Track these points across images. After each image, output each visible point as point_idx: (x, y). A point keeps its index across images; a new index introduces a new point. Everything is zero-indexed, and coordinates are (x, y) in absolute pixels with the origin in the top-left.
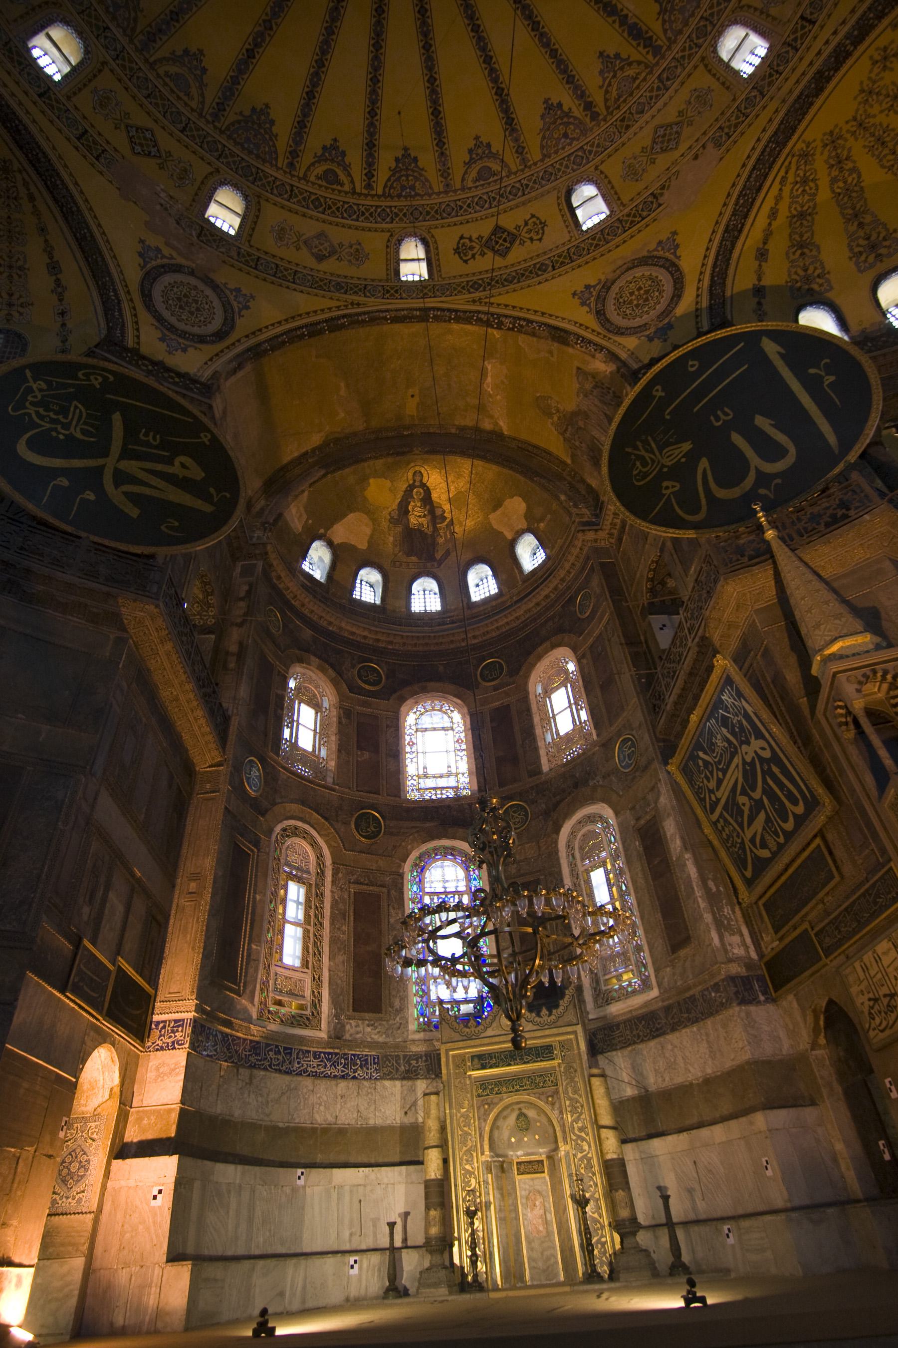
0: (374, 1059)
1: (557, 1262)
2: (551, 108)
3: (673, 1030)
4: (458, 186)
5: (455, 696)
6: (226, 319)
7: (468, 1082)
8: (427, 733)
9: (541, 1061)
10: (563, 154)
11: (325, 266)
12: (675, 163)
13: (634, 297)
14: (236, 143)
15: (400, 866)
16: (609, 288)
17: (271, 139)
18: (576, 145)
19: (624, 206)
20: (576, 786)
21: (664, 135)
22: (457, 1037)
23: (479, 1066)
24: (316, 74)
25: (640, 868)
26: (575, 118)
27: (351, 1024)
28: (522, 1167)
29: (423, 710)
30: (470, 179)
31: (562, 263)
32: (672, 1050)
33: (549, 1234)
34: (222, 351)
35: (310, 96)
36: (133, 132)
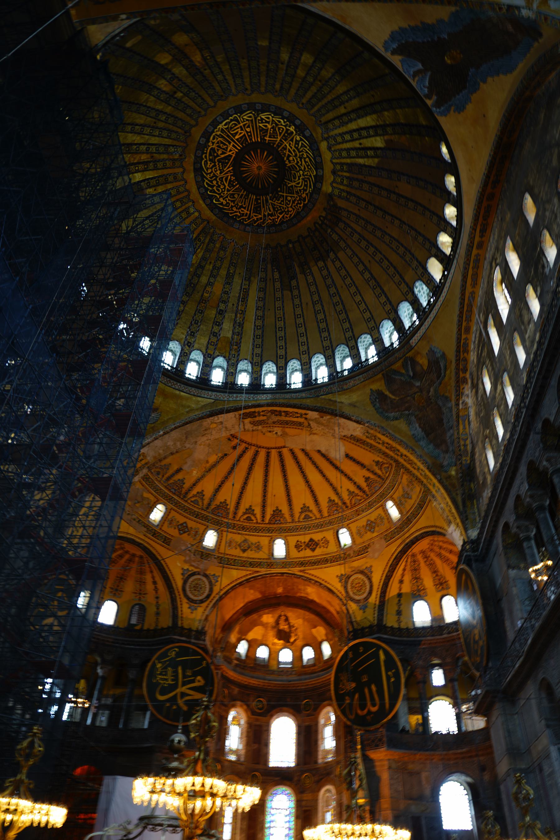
2: (330, 500)
4: (297, 520)
11: (245, 555)
18: (340, 514)
24: (244, 487)
35: (241, 493)
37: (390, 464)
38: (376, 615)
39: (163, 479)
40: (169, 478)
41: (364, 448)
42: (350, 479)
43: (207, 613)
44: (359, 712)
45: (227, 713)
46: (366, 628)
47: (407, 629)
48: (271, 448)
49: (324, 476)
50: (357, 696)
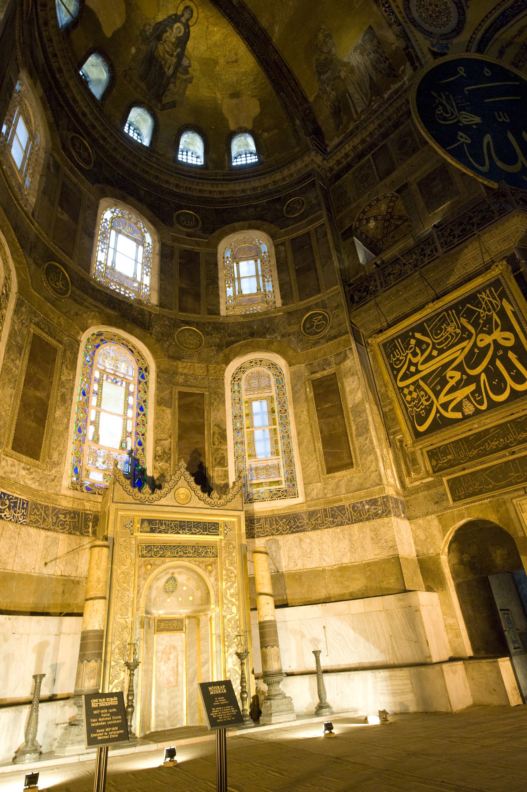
0: (23, 504)
1: (182, 709)
3: (314, 529)
5: (150, 221)
7: (133, 542)
8: (120, 236)
9: (207, 534)
13: (430, 8)
20: (252, 335)
22: (130, 499)
23: (148, 529)
25: (306, 407)
27: (7, 461)
28: (163, 624)
29: (120, 215)
32: (310, 544)
33: (177, 684)
50: (488, 138)
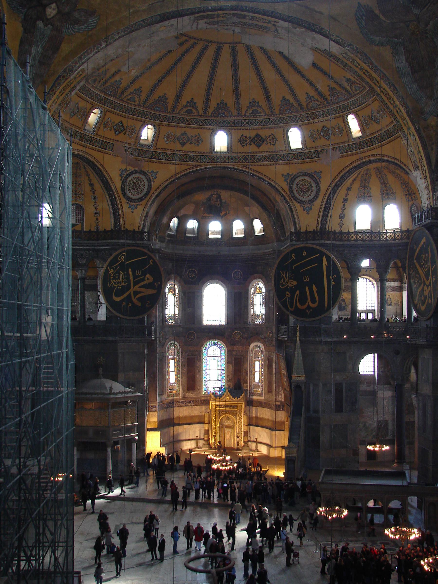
2: (284, 99)
4: (243, 114)
6: (149, 185)
10: (287, 115)
11: (185, 148)
12: (326, 145)
14: (152, 109)
15: (201, 349)
16: (295, 179)
17: (166, 104)
19: (307, 148)
20: (257, 334)
21: (325, 131)
26: (294, 106)
30: (249, 112)
31: (281, 159)
34: (148, 201)
36: (116, 127)
37: (365, 87)
38: (320, 220)
39: (100, 85)
40: (106, 82)
41: (337, 64)
42: (311, 84)
43: (146, 210)
44: (298, 305)
45: (165, 287)
46: (310, 232)
47: (349, 233)
48: (224, 43)
49: (282, 76)
50: (298, 292)
